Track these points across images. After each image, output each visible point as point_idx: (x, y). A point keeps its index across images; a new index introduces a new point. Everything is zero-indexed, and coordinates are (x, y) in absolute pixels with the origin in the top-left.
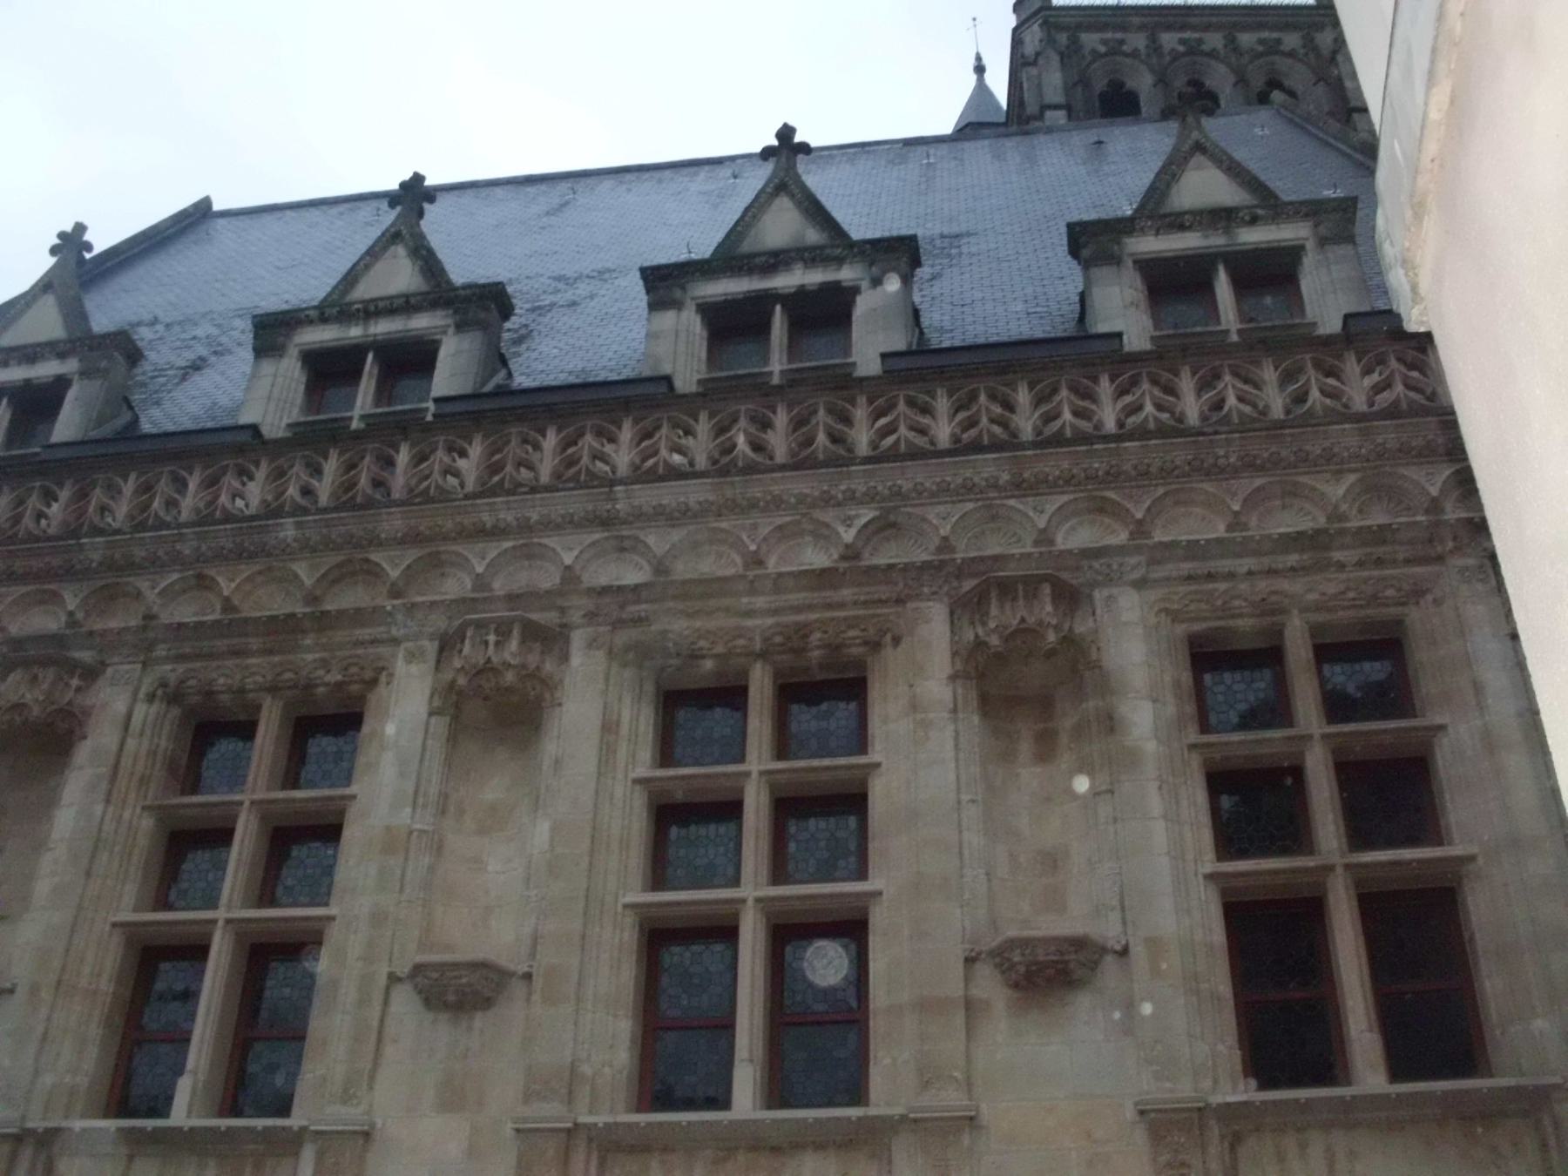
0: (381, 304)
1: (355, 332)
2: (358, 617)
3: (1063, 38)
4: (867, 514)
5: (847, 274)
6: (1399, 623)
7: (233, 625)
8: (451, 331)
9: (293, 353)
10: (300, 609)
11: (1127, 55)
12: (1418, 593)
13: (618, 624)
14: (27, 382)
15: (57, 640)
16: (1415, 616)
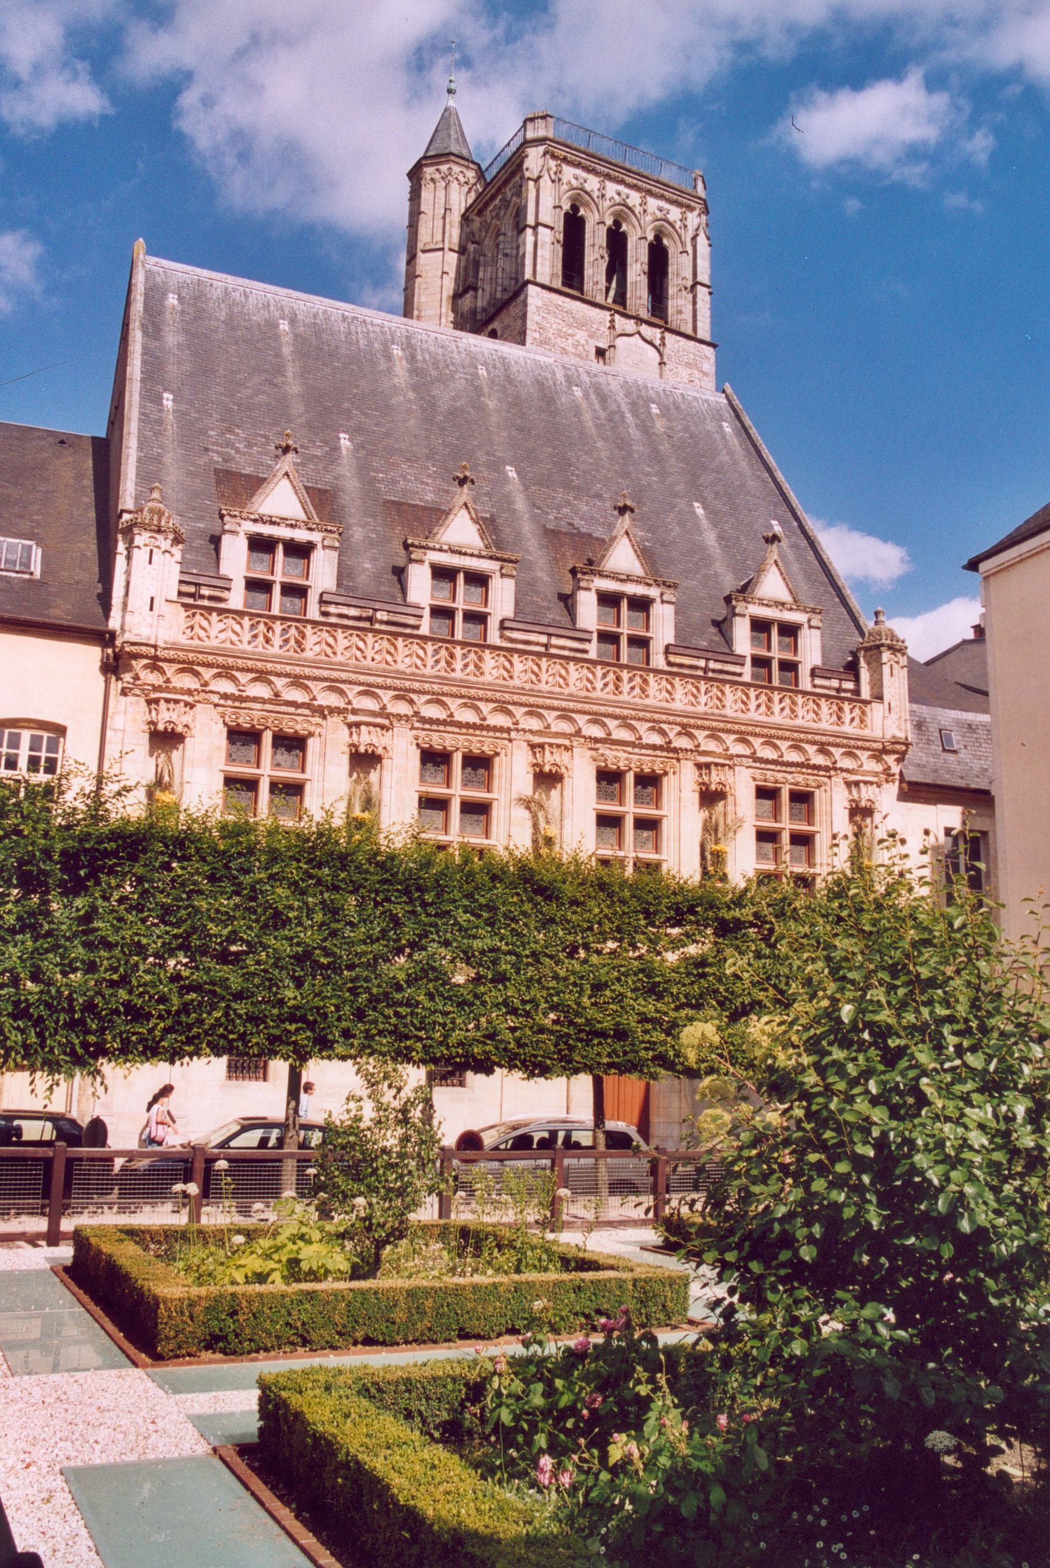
0: (469, 551)
1: (455, 561)
2: (501, 729)
3: (552, 164)
4: (678, 729)
5: (653, 592)
6: (812, 794)
7: (450, 722)
8: (498, 574)
9: (427, 563)
10: (478, 722)
11: (586, 192)
12: (819, 787)
13: (591, 749)
14: (292, 540)
15: (373, 714)
16: (817, 792)
